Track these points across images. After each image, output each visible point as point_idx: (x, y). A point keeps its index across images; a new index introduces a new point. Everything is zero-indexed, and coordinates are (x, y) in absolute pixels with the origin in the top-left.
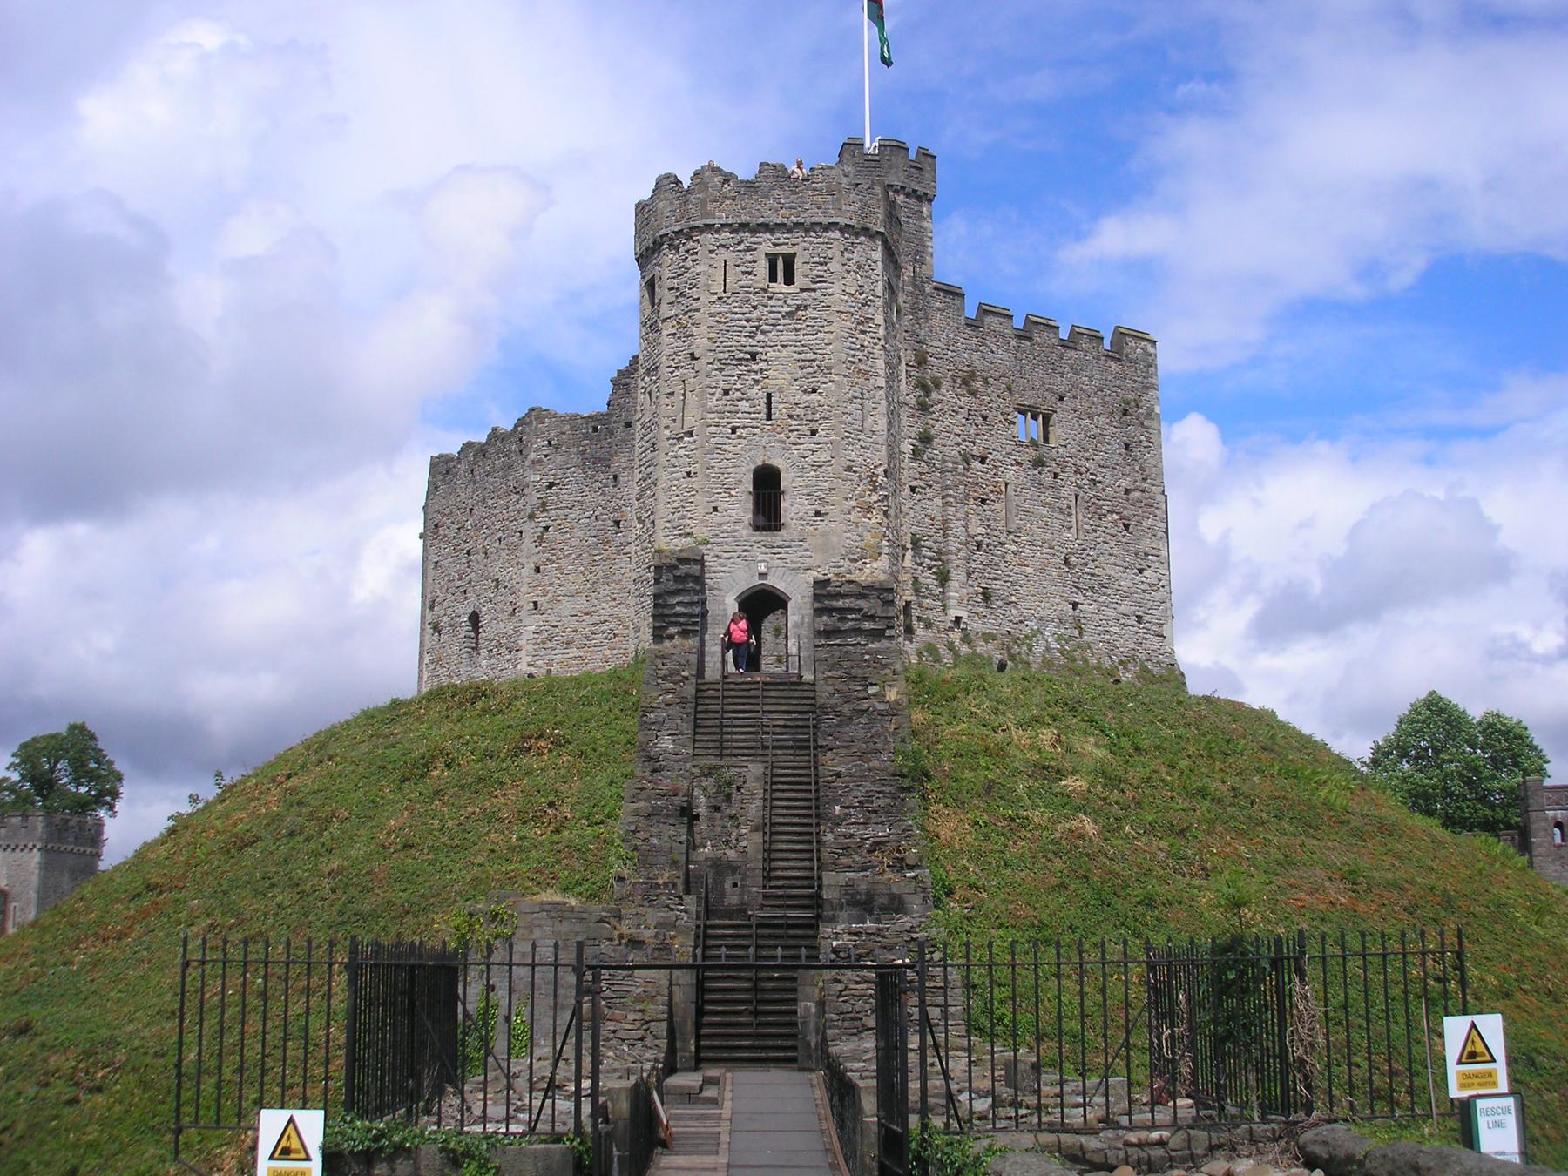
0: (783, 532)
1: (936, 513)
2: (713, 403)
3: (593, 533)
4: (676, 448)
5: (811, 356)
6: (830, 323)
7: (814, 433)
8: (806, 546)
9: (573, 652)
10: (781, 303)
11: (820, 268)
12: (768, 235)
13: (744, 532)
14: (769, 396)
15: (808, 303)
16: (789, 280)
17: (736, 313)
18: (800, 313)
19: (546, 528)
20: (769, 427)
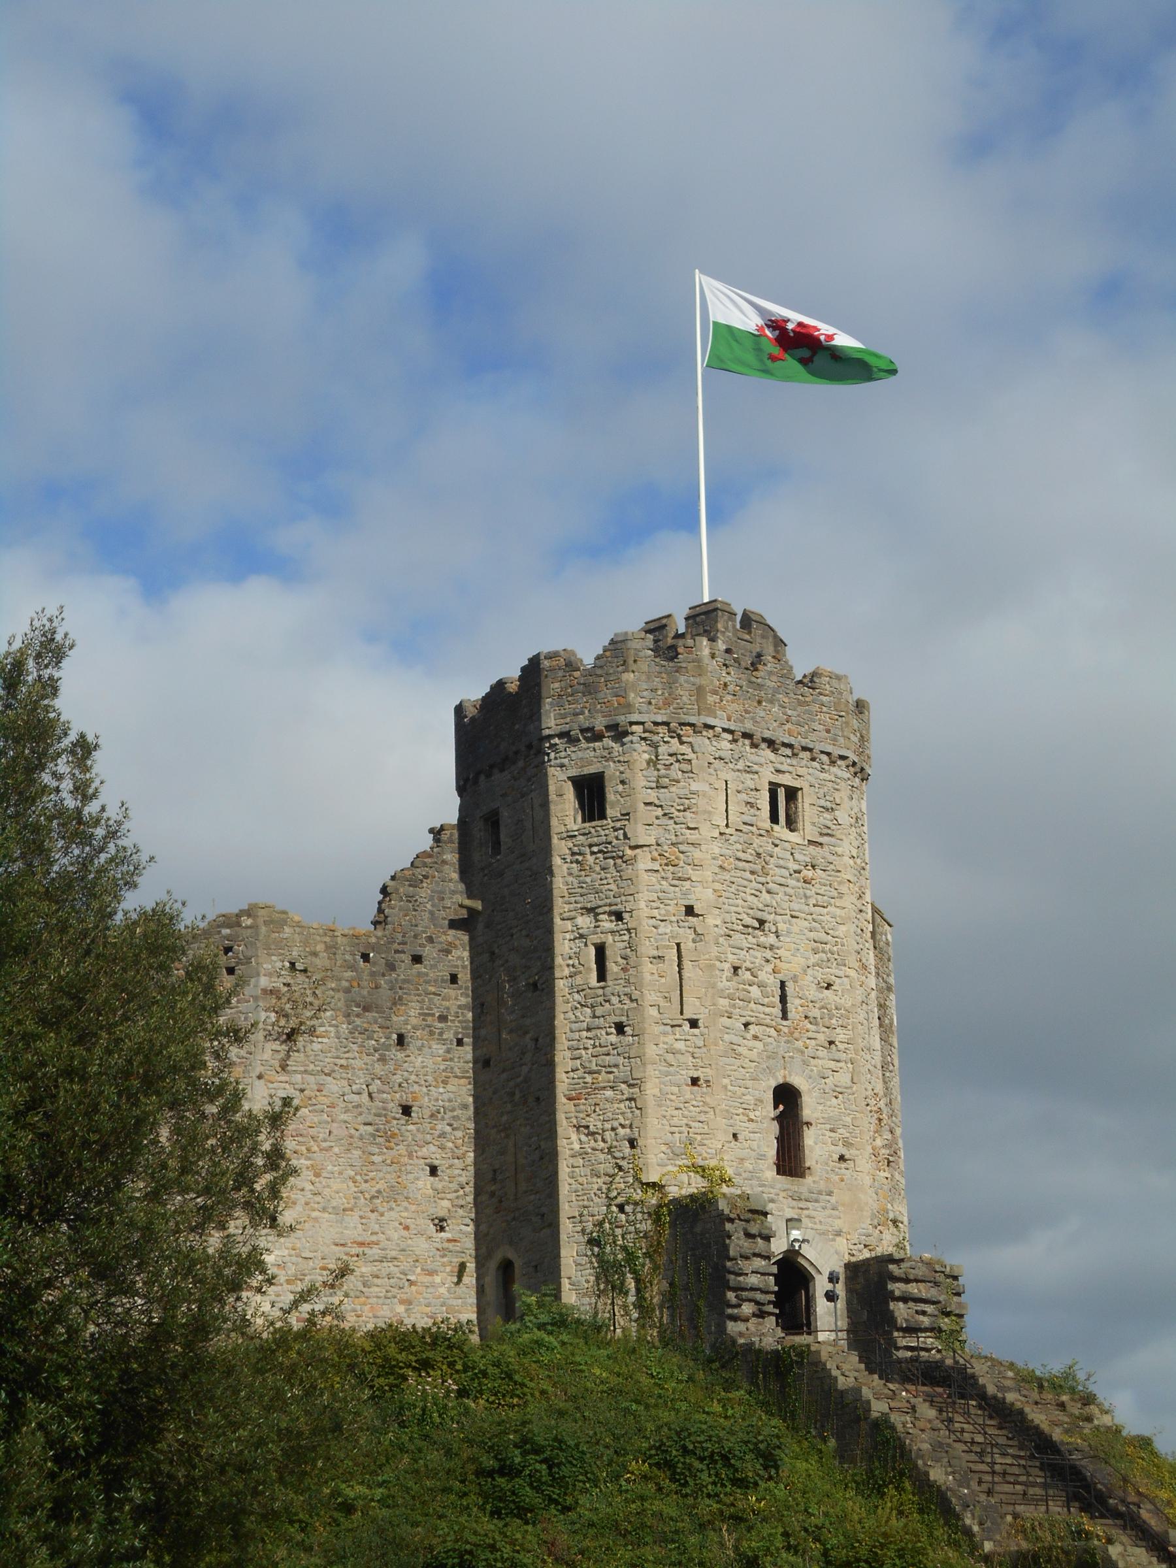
0: (809, 1180)
2: (725, 982)
3: (370, 1119)
4: (670, 1039)
5: (822, 936)
6: (841, 895)
7: (831, 1043)
11: (826, 815)
12: (772, 756)
14: (783, 984)
15: (818, 862)
16: (791, 824)
17: (739, 860)
18: (809, 874)
20: (786, 1030)
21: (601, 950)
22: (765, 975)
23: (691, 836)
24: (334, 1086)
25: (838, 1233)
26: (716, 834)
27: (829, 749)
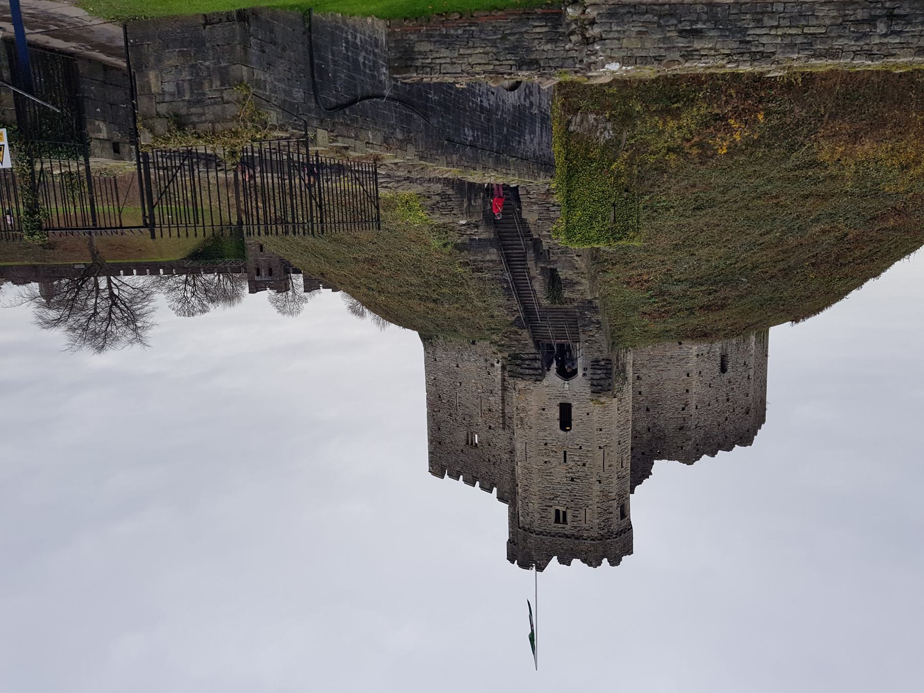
0: (558, 402)
1: (507, 407)
4: (607, 442)
5: (548, 477)
6: (539, 491)
7: (546, 444)
8: (548, 396)
9: (669, 354)
10: (561, 502)
12: (566, 532)
13: (575, 403)
14: (565, 461)
16: (557, 511)
18: (552, 496)
19: (683, 409)
21: (622, 467)
22: (571, 464)
23: (599, 505)
24: (669, 415)
25: (547, 386)
26: (590, 507)
27: (543, 537)
